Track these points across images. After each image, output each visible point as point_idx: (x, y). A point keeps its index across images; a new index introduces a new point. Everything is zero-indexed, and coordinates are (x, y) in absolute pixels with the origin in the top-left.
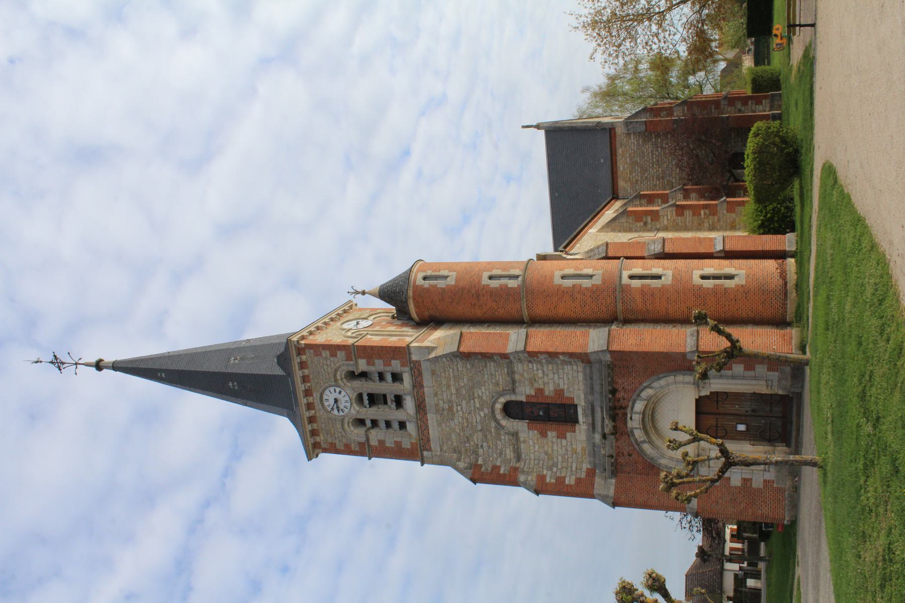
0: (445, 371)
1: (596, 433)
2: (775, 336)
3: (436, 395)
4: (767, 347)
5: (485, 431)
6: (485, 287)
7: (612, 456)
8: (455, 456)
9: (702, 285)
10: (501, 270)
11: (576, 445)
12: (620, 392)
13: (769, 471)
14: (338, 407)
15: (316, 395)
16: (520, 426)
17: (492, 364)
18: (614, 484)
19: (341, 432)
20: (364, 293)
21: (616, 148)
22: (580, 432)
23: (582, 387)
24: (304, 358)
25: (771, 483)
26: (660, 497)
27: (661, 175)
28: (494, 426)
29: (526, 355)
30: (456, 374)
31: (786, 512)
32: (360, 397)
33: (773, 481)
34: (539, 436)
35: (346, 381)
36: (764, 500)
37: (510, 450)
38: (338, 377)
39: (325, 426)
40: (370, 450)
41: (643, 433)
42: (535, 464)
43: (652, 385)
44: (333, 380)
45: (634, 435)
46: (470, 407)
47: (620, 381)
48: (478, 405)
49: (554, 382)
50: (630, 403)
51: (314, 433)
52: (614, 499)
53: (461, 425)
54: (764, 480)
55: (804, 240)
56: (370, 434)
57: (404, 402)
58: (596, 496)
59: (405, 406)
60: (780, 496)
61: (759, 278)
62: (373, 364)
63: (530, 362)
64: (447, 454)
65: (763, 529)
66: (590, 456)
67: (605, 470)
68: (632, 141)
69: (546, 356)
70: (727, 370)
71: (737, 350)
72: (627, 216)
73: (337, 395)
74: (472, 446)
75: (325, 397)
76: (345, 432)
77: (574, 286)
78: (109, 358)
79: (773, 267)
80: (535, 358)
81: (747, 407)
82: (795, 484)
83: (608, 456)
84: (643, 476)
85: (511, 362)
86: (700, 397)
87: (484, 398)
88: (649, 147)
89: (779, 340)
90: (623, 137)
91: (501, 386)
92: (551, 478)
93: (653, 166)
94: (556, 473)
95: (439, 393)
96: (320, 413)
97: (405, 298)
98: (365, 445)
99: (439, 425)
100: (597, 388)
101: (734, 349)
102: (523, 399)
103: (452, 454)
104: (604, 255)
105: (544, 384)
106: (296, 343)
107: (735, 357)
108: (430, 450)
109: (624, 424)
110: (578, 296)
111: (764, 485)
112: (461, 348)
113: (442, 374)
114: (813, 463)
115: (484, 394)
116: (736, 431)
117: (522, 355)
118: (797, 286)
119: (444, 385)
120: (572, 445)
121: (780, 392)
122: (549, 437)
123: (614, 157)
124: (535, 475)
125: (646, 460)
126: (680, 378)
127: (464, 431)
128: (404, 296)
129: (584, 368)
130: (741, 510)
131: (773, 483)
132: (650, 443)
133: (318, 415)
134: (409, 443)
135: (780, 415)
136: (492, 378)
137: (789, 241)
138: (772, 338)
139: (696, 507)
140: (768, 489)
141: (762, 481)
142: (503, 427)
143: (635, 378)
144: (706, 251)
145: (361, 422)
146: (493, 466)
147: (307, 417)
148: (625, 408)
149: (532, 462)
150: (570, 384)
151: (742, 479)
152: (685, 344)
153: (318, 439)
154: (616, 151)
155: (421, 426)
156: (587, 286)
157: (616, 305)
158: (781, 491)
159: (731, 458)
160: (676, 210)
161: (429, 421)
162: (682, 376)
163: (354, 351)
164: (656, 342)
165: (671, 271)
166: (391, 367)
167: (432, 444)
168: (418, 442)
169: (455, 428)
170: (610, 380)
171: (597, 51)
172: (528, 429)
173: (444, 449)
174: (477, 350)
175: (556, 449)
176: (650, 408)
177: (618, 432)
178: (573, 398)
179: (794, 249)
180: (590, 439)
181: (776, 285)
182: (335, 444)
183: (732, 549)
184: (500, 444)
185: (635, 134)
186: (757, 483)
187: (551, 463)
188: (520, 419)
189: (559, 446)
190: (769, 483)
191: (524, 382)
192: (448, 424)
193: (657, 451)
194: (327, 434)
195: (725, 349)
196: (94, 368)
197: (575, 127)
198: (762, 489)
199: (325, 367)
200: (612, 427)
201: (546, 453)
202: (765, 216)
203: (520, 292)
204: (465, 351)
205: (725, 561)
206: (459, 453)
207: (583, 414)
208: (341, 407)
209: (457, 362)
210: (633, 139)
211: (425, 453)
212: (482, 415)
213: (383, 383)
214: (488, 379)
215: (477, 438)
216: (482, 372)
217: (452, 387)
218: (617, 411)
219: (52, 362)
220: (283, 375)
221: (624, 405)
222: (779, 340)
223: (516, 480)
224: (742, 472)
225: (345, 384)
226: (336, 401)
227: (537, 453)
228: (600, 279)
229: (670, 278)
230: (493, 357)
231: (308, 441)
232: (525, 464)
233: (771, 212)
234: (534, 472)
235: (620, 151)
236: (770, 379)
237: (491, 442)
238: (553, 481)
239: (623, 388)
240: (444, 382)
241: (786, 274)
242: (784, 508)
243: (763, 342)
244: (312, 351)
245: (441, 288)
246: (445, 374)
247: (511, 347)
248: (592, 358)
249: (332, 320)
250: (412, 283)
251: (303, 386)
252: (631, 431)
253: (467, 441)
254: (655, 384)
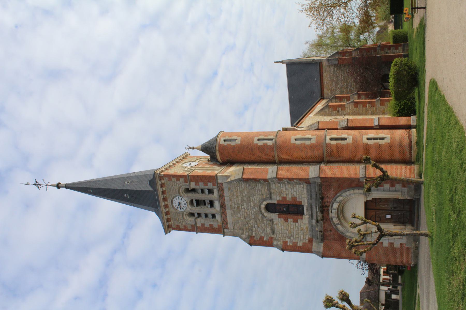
0: (235, 188)
1: (313, 219)
2: (405, 169)
3: (231, 200)
4: (402, 175)
5: (256, 219)
6: (256, 145)
7: (321, 231)
8: (241, 231)
9: (368, 143)
10: (264, 136)
11: (303, 226)
12: (325, 198)
13: (403, 239)
14: (180, 207)
15: (169, 201)
16: (274, 216)
17: (260, 184)
18: (323, 246)
19: (182, 220)
20: (193, 148)
21: (322, 73)
22: (305, 219)
23: (306, 196)
24: (163, 181)
25: (404, 245)
26: (346, 252)
27: (346, 87)
28: (260, 216)
29: (277, 179)
30: (241, 189)
31: (412, 260)
32: (192, 202)
33: (405, 244)
34: (284, 221)
35: (184, 193)
36: (400, 254)
37: (269, 228)
38: (181, 191)
39: (174, 216)
40: (197, 229)
41: (338, 220)
42: (282, 236)
43: (342, 195)
44: (178, 193)
45: (332, 220)
46: (248, 206)
47: (326, 193)
48: (252, 206)
49: (291, 193)
50: (331, 204)
51: (168, 220)
52: (323, 254)
53: (244, 216)
54: (400, 243)
55: (420, 120)
56: (197, 221)
57: (214, 204)
58: (313, 252)
59: (215, 206)
60: (409, 251)
61: (397, 139)
62: (199, 185)
63: (279, 183)
64: (237, 231)
65: (400, 269)
66: (310, 231)
67: (318, 238)
68: (331, 69)
69: (287, 180)
70: (381, 187)
71: (386, 176)
72: (329, 107)
73: (180, 201)
74: (249, 226)
75: (174, 202)
76: (184, 220)
77: (301, 144)
78: (63, 182)
79: (405, 133)
80: (282, 181)
81: (391, 206)
82: (416, 245)
83: (320, 232)
84: (338, 242)
85: (269, 183)
86: (367, 201)
87: (256, 202)
88: (339, 72)
89: (408, 171)
90: (326, 67)
91: (264, 196)
92: (290, 243)
93: (342, 82)
94: (293, 240)
95: (232, 199)
96: (171, 210)
97: (215, 151)
98: (194, 226)
99: (232, 216)
100: (314, 196)
101: (384, 176)
102: (276, 202)
103: (239, 231)
104: (317, 128)
105: (286, 194)
106: (159, 174)
107: (385, 180)
108: (228, 228)
109: (328, 215)
110: (303, 149)
111: (400, 246)
112: (244, 176)
113: (234, 190)
114: (426, 235)
115: (255, 200)
116: (386, 218)
117: (275, 179)
118: (417, 143)
119: (235, 195)
120: (301, 226)
121: (409, 198)
122: (289, 222)
123: (322, 77)
124: (282, 241)
125: (339, 233)
126: (356, 191)
127: (245, 219)
128: (214, 150)
129: (307, 186)
130: (388, 259)
131: (405, 245)
132: (341, 224)
133: (170, 211)
134: (217, 225)
135: (408, 210)
136: (259, 192)
137: (413, 120)
138: (404, 170)
139: (365, 258)
140: (403, 248)
141: (400, 244)
142: (265, 217)
143: (333, 191)
144: (369, 126)
145: (192, 214)
146: (260, 237)
147: (165, 212)
148: (328, 207)
149: (280, 234)
150: (300, 194)
151: (389, 243)
152: (359, 173)
153: (170, 223)
154: (323, 74)
155: (223, 216)
156: (308, 144)
157: (323, 154)
158: (409, 249)
159: (383, 232)
160: (354, 105)
161: (227, 214)
162: (357, 190)
163: (189, 178)
164: (344, 172)
165: (352, 136)
166: (207, 186)
167: (228, 225)
168: (222, 224)
169: (241, 218)
170: (320, 192)
171: (313, 23)
172: (278, 218)
173: (235, 228)
174: (252, 177)
175: (293, 228)
176: (341, 207)
177: (325, 219)
178: (301, 202)
179: (415, 124)
180: (310, 222)
181: (406, 143)
182: (179, 226)
183: (384, 279)
184: (264, 225)
185: (332, 65)
186: (397, 245)
187: (290, 235)
188: (274, 212)
189: (294, 226)
190: (403, 245)
191: (276, 194)
192: (237, 215)
193: (345, 229)
194: (175, 221)
195: (380, 176)
196: (56, 187)
197: (301, 62)
198: (399, 248)
199: (174, 186)
200: (321, 217)
201: (288, 230)
202: (400, 107)
203: (274, 147)
204: (246, 178)
205: (380, 285)
206: (243, 230)
207: (306, 210)
208: (182, 207)
209: (242, 183)
210: (331, 68)
211: (225, 230)
212: (255, 211)
213: (203, 195)
214: (258, 192)
215: (252, 222)
216: (254, 188)
217: (239, 196)
218: (324, 208)
219: (34, 184)
220: (152, 191)
221: (327, 205)
222: (408, 171)
223: (272, 244)
224: (389, 240)
225: (184, 195)
226: (179, 204)
227: (283, 230)
228: (315, 140)
229: (351, 140)
230: (260, 181)
231: (165, 224)
232: (277, 236)
233: (403, 105)
234: (281, 240)
235: (325, 74)
236: (403, 191)
237: (259, 225)
238: (291, 244)
239: (327, 196)
240: (235, 194)
241: (411, 137)
242: (411, 258)
243: (399, 172)
244: (167, 178)
245: (233, 146)
246: (235, 189)
247: (269, 176)
248: (311, 181)
249: (177, 162)
250: (218, 143)
251: (162, 196)
252: (331, 218)
253: (247, 224)
254: (344, 194)
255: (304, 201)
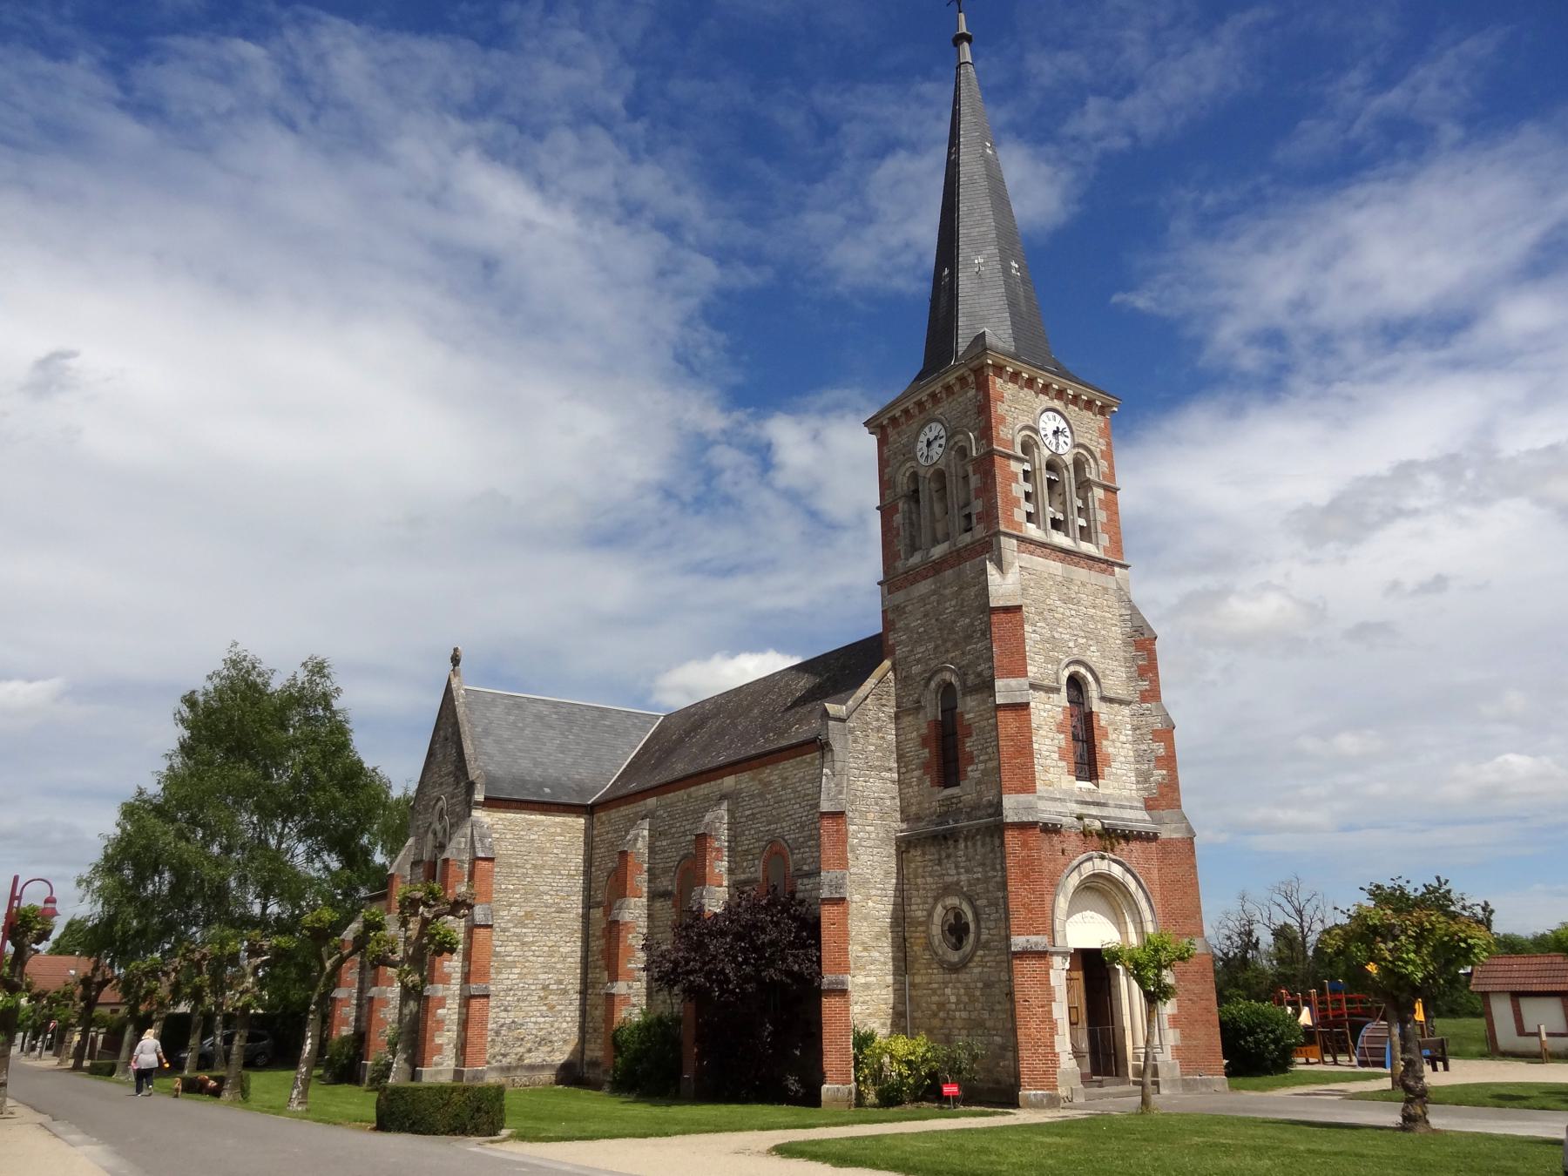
255: (1107, 787)
